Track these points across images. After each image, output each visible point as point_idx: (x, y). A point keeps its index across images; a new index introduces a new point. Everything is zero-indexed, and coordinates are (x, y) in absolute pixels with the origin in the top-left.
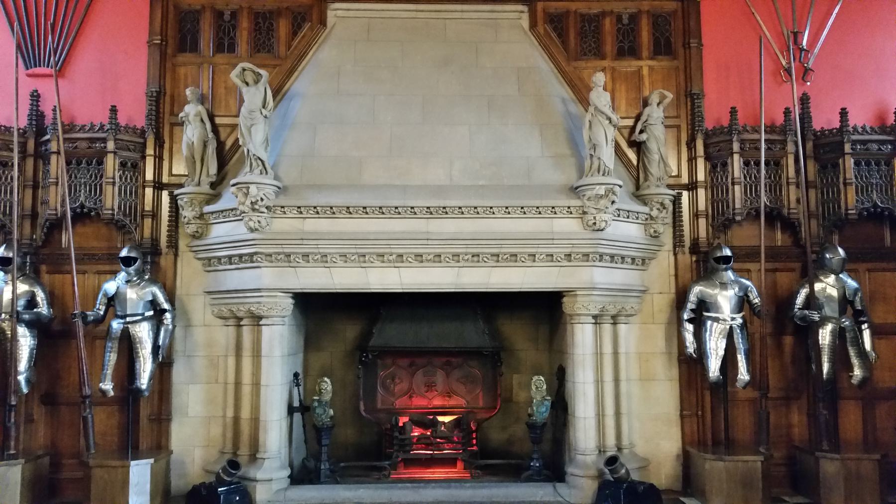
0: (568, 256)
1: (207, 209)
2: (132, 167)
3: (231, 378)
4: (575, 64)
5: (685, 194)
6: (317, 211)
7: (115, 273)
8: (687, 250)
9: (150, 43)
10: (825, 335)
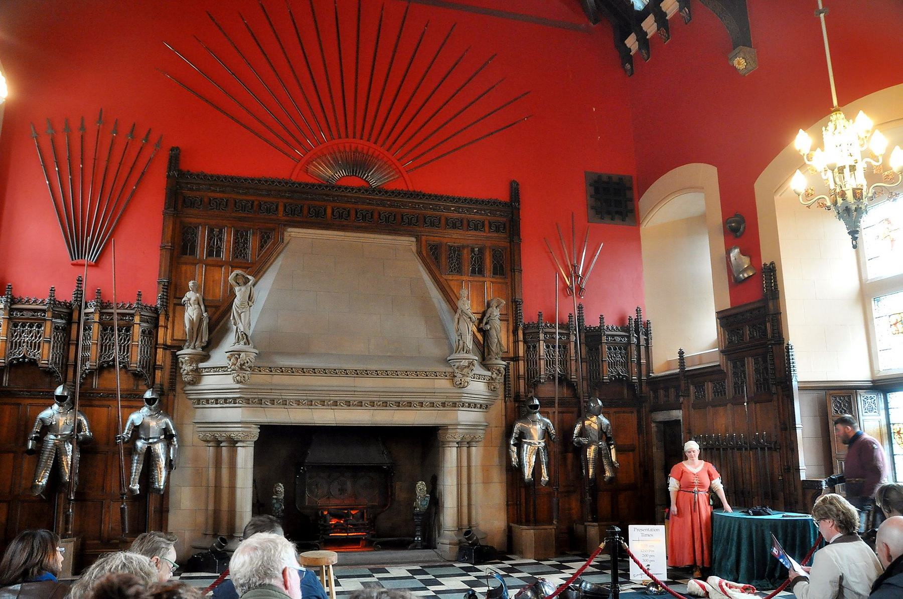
0: (443, 405)
1: (201, 365)
2: (150, 334)
3: (212, 483)
4: (445, 277)
5: (512, 363)
6: (282, 370)
7: (139, 408)
8: (512, 399)
9: (163, 248)
10: (591, 453)
